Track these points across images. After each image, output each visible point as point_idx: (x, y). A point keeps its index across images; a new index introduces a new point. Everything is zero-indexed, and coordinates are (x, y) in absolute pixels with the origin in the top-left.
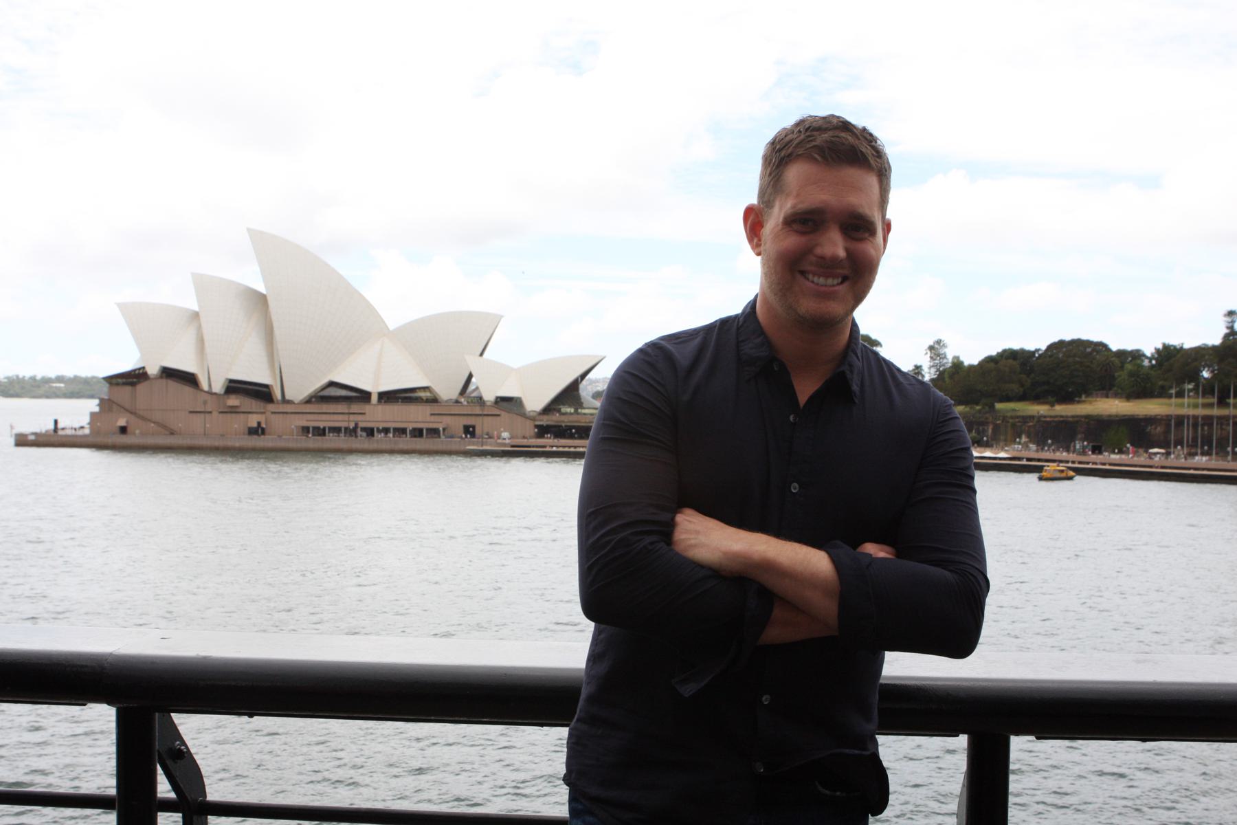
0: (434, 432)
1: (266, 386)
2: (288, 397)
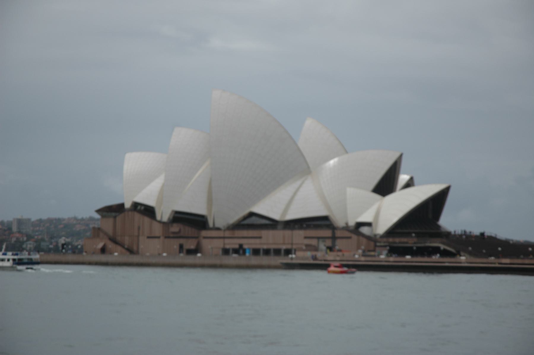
1: (203, 216)
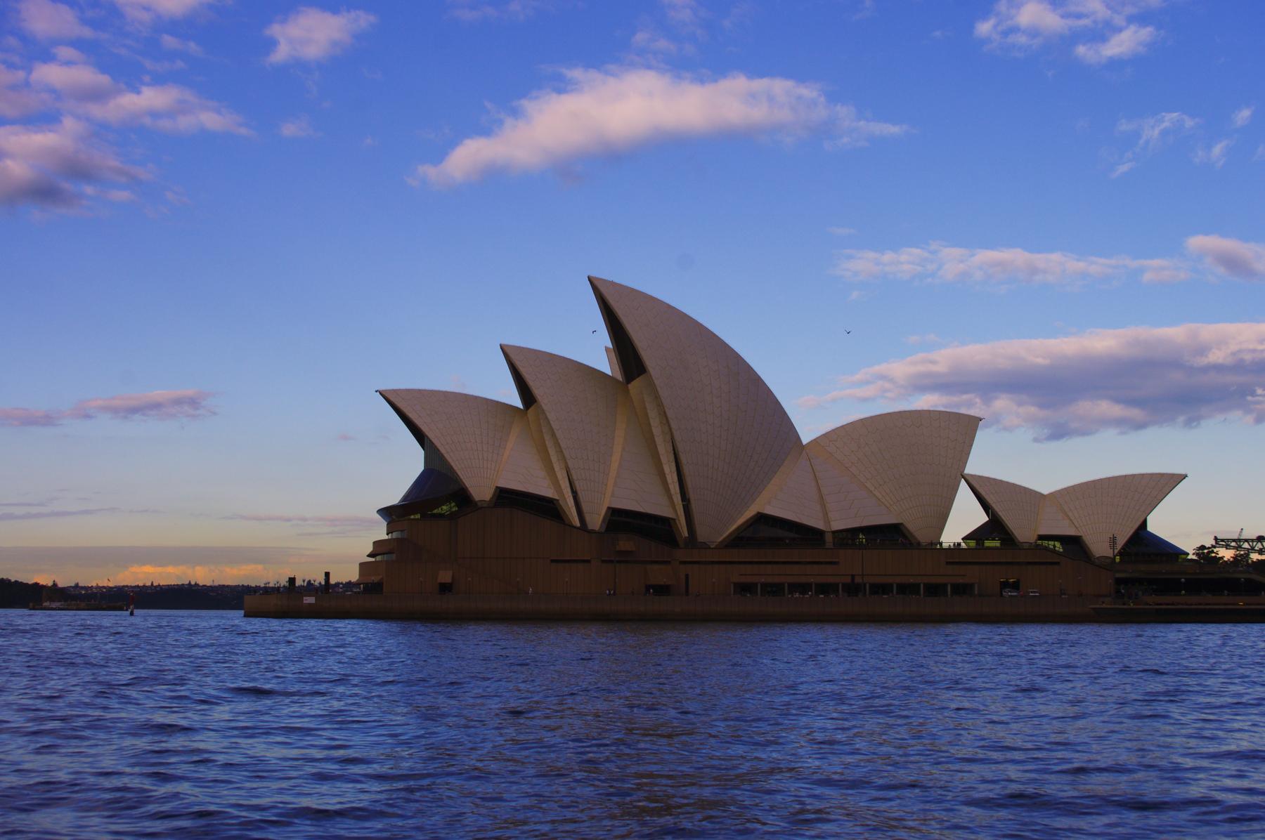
0: (962, 590)
2: (702, 534)
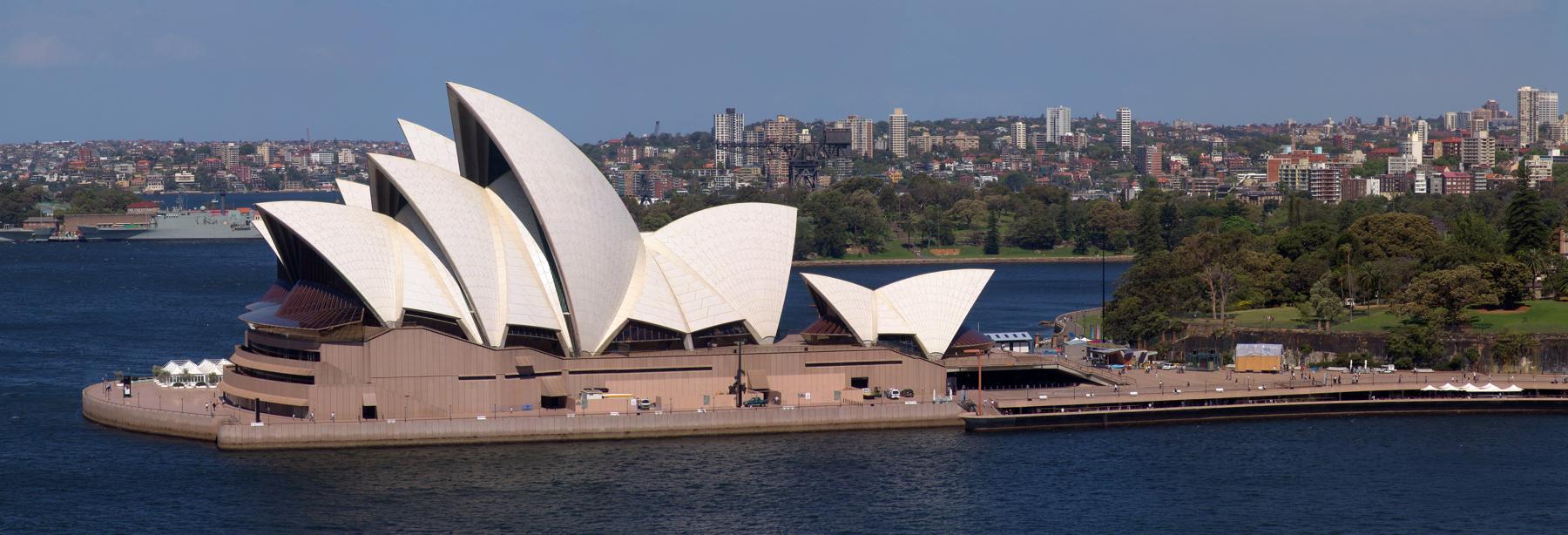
1: (552, 333)
2: (584, 345)
